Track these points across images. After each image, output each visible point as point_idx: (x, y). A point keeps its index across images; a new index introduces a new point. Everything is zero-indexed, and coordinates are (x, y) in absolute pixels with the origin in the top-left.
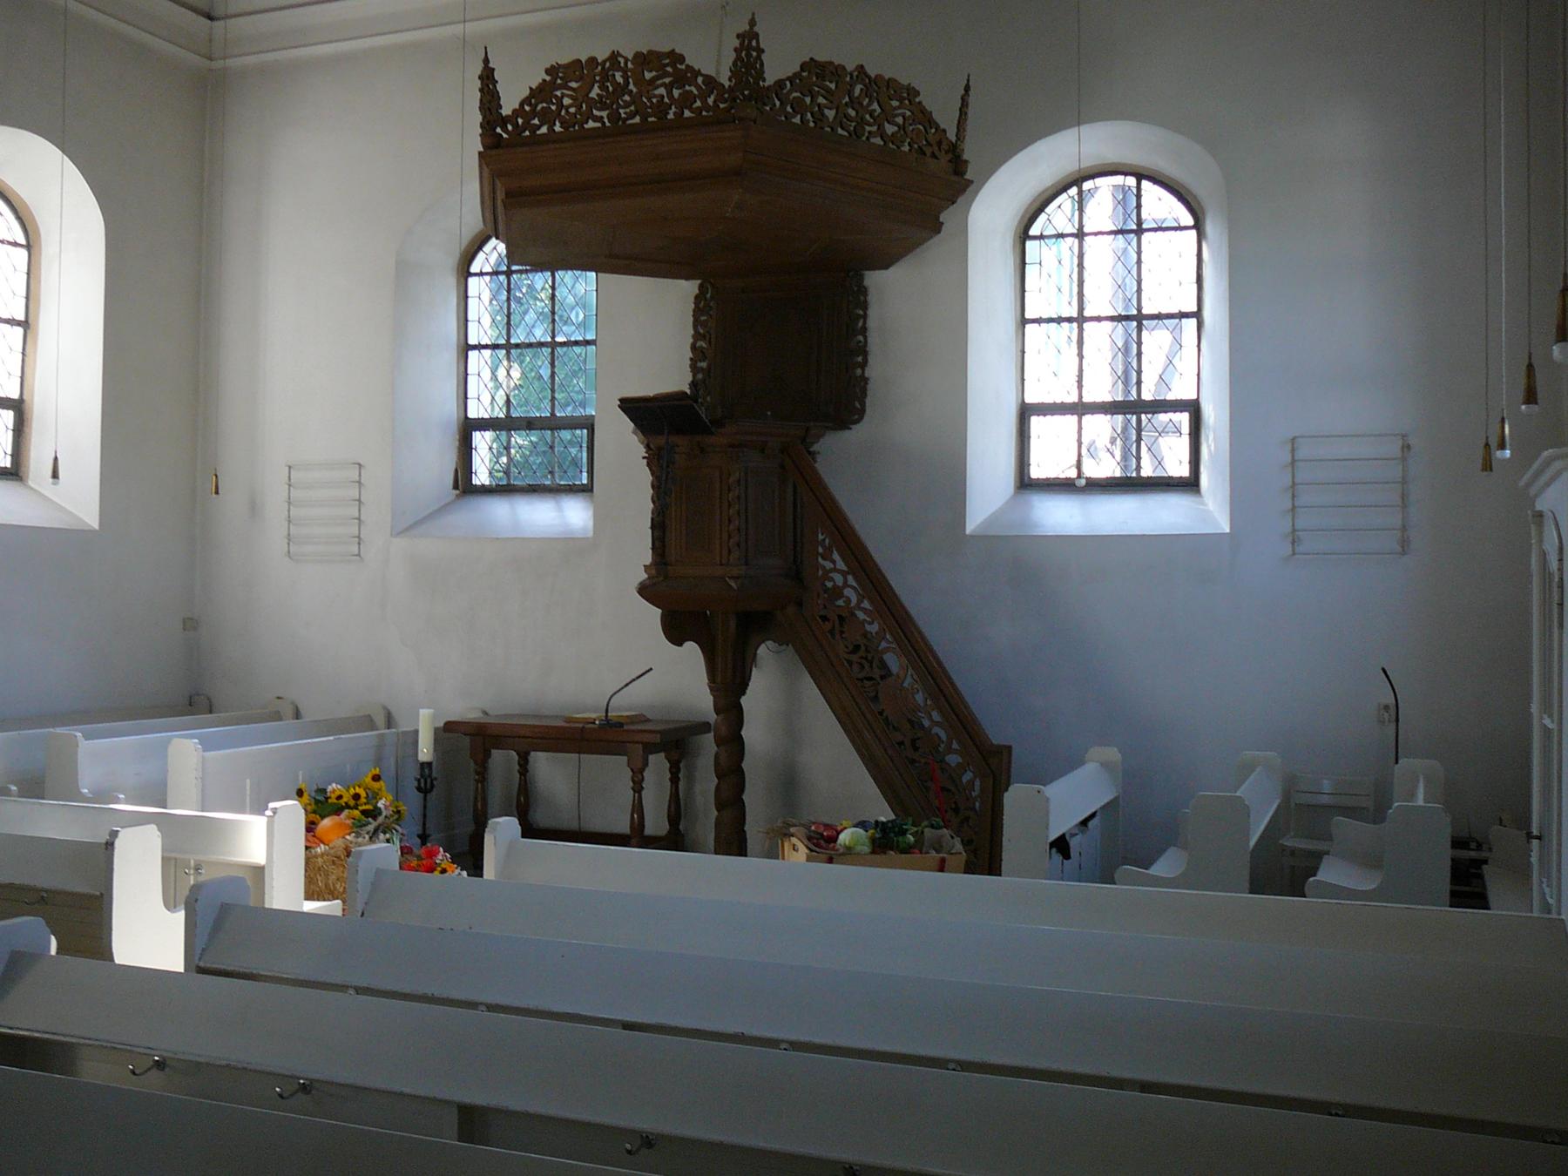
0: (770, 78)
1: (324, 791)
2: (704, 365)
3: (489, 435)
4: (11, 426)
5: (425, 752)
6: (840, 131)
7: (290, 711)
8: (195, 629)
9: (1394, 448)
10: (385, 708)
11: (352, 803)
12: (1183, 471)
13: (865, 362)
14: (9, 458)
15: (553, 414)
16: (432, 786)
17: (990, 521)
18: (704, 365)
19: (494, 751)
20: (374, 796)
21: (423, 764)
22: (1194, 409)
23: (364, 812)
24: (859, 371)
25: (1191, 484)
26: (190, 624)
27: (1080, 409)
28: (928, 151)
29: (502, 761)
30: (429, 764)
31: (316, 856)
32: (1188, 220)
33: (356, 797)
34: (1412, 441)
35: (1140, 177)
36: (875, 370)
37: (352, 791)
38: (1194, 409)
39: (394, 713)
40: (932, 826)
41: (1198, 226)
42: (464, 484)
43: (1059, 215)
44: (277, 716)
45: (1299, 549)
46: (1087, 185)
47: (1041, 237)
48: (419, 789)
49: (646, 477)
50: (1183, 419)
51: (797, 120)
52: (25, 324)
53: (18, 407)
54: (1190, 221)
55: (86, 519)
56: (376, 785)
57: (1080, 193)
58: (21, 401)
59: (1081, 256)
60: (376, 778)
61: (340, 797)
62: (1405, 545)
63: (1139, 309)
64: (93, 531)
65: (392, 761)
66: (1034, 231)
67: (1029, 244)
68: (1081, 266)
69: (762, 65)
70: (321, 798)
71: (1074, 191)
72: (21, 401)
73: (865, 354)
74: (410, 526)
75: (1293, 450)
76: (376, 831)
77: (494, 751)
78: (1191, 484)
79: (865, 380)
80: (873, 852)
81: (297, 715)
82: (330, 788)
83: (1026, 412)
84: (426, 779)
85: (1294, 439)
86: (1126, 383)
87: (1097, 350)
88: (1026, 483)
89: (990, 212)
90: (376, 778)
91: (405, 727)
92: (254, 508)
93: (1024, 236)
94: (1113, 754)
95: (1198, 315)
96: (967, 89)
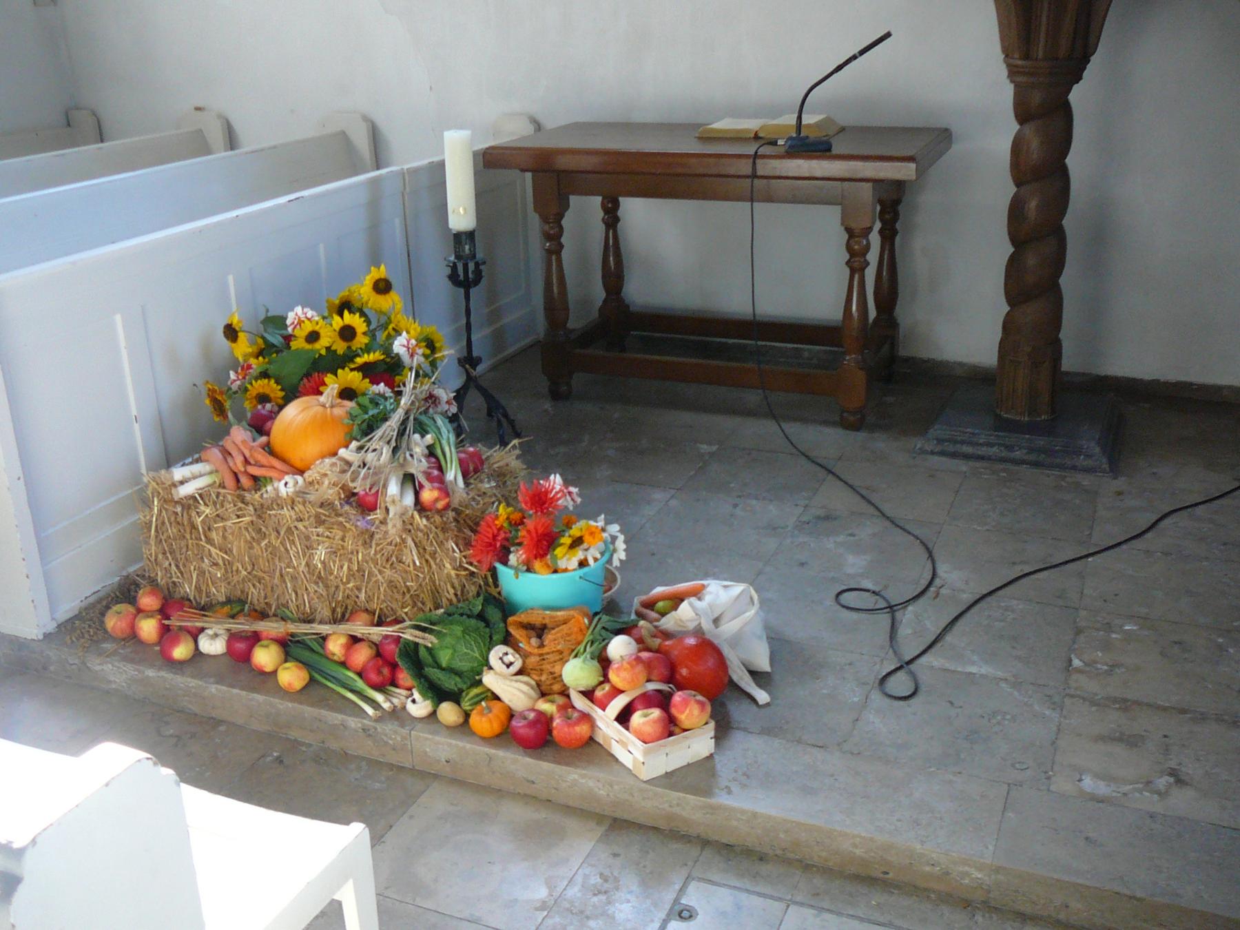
1: (278, 322)
5: (461, 216)
7: (216, 135)
10: (366, 119)
11: (340, 347)
19: (573, 199)
20: (383, 327)
21: (458, 237)
23: (368, 371)
29: (585, 211)
30: (470, 235)
31: (277, 502)
33: (347, 333)
37: (337, 322)
44: (198, 145)
48: (453, 277)
56: (385, 302)
60: (382, 287)
61: (313, 337)
65: (398, 222)
70: (276, 340)
76: (401, 433)
77: (573, 199)
81: (232, 141)
82: (291, 318)
84: (468, 265)
90: (382, 287)
91: (407, 157)
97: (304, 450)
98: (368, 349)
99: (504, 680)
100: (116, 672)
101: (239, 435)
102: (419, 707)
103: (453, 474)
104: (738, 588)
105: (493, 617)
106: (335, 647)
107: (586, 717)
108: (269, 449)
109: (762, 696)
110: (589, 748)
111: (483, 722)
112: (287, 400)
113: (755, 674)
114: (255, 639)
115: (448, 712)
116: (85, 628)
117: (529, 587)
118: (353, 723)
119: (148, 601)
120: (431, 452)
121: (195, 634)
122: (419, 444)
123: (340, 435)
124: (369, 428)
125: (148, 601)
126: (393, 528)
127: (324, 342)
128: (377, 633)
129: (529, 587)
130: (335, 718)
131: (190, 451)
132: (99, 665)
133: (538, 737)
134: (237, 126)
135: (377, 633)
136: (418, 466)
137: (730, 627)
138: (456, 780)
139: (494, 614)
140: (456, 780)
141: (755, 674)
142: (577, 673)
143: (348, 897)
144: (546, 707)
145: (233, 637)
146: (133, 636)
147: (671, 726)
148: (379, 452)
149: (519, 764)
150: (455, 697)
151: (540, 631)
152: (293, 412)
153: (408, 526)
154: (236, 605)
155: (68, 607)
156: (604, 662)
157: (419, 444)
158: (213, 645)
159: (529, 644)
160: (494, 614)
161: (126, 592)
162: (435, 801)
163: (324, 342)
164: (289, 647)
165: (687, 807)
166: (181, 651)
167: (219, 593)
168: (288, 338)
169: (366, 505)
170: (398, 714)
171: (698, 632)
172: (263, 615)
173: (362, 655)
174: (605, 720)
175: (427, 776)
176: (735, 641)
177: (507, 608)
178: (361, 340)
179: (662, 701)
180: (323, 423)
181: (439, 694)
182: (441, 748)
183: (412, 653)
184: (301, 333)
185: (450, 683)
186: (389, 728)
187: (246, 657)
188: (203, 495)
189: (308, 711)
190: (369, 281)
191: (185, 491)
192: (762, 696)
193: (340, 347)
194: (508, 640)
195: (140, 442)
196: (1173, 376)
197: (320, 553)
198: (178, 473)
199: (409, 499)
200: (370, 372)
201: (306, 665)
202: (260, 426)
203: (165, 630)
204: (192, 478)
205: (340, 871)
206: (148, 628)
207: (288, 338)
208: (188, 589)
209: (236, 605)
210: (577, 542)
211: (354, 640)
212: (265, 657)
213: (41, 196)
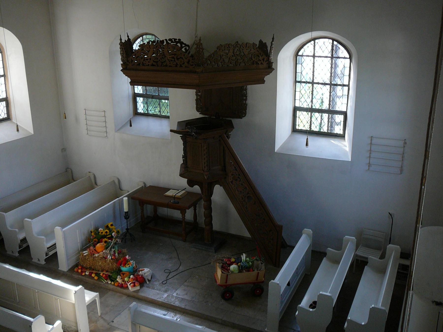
0: (206, 55)
2: (200, 94)
3: (142, 99)
4: (5, 106)
6: (231, 65)
8: (65, 151)
9: (401, 143)
12: (341, 132)
13: (246, 100)
14: (6, 115)
15: (159, 95)
16: (129, 217)
17: (282, 147)
18: (200, 94)
21: (126, 212)
22: (345, 114)
24: (244, 102)
25: (342, 136)
26: (64, 150)
27: (311, 110)
28: (259, 63)
32: (348, 56)
34: (407, 141)
35: (333, 40)
36: (249, 101)
38: (345, 114)
39: (120, 179)
40: (257, 260)
41: (350, 58)
42: (136, 113)
43: (308, 49)
45: (371, 168)
46: (317, 41)
47: (302, 56)
48: (125, 218)
49: (182, 142)
50: (341, 117)
51: (216, 66)
52: (4, 76)
53: (6, 100)
54: (348, 56)
55: (30, 131)
57: (314, 43)
58: (7, 98)
59: (314, 64)
60: (112, 225)
61: (102, 233)
62: (401, 171)
63: (330, 87)
64: (32, 135)
65: (118, 207)
66: (300, 53)
67: (298, 57)
68: (314, 66)
69: (203, 54)
71: (313, 42)
72: (7, 98)
73: (246, 97)
74: (119, 129)
75: (371, 140)
76: (111, 248)
78: (342, 136)
79: (246, 105)
80: (239, 272)
83: (296, 109)
85: (372, 137)
86: (336, 64)
87: (317, 94)
88: (295, 130)
89: (284, 58)
92: (77, 120)
93: (297, 55)
94: (310, 231)
95: (348, 86)
96: (273, 39)
97: (99, 250)
98: (109, 235)
99: (119, 280)
100: (76, 276)
101: (92, 248)
102: (110, 282)
103: (116, 254)
104: (148, 269)
105: (119, 272)
106: (101, 274)
107: (127, 284)
108: (95, 250)
109: (148, 283)
110: (127, 287)
111: (116, 284)
112: (98, 243)
113: (149, 280)
114: (92, 273)
115: (113, 283)
116: (72, 270)
117: (124, 269)
118: (103, 284)
119: (80, 267)
120: (114, 251)
121: (85, 272)
122: (113, 250)
123: (103, 249)
124: (107, 248)
125: (80, 267)
126: (108, 261)
127: (103, 234)
128: (106, 273)
129: (124, 269)
130: (100, 283)
131: (85, 249)
132: (73, 275)
133: (121, 286)
134: (96, 176)
135: (106, 273)
136: (112, 253)
137: (146, 275)
138: (113, 290)
139: (119, 272)
140: (113, 290)
141: (149, 280)
142: (126, 279)
143: (97, 299)
144: (123, 283)
145: (90, 273)
146: (78, 271)
147: (134, 286)
148: (108, 251)
149: (119, 289)
150: (114, 281)
151: (124, 274)
152: (98, 245)
153: (110, 261)
154: (90, 268)
155: (70, 267)
156: (130, 278)
157: (113, 250)
158: (87, 273)
159: (122, 276)
160: (119, 272)
161: (77, 265)
162: (110, 293)
163: (103, 234)
164: (96, 274)
165: (135, 294)
166: (83, 274)
167: (89, 267)
168: (99, 232)
169: (106, 258)
170: (107, 283)
171: (142, 275)
172: (93, 270)
173: (104, 276)
174: (128, 284)
175: (110, 290)
176: (147, 276)
177: (121, 271)
178: (108, 233)
179: (134, 283)
180: (102, 247)
181: (112, 281)
182: (111, 287)
183: (109, 276)
184: (101, 232)
185: (113, 280)
186: (106, 284)
187: (91, 275)
188: (87, 255)
189: (98, 282)
190: (110, 224)
191: (85, 254)
192: (148, 283)
193: (105, 234)
194: (120, 275)
195: (79, 245)
196: (239, 234)
197: (100, 263)
198: (84, 252)
199: (110, 258)
200: (109, 238)
201: (98, 276)
202: (94, 246)
203: (82, 271)
204: (86, 253)
205: (96, 296)
206: (80, 271)
207: (99, 232)
208: (85, 266)
209: (90, 268)
210: (128, 264)
211: (104, 274)
212: (93, 275)
213: (71, 227)
